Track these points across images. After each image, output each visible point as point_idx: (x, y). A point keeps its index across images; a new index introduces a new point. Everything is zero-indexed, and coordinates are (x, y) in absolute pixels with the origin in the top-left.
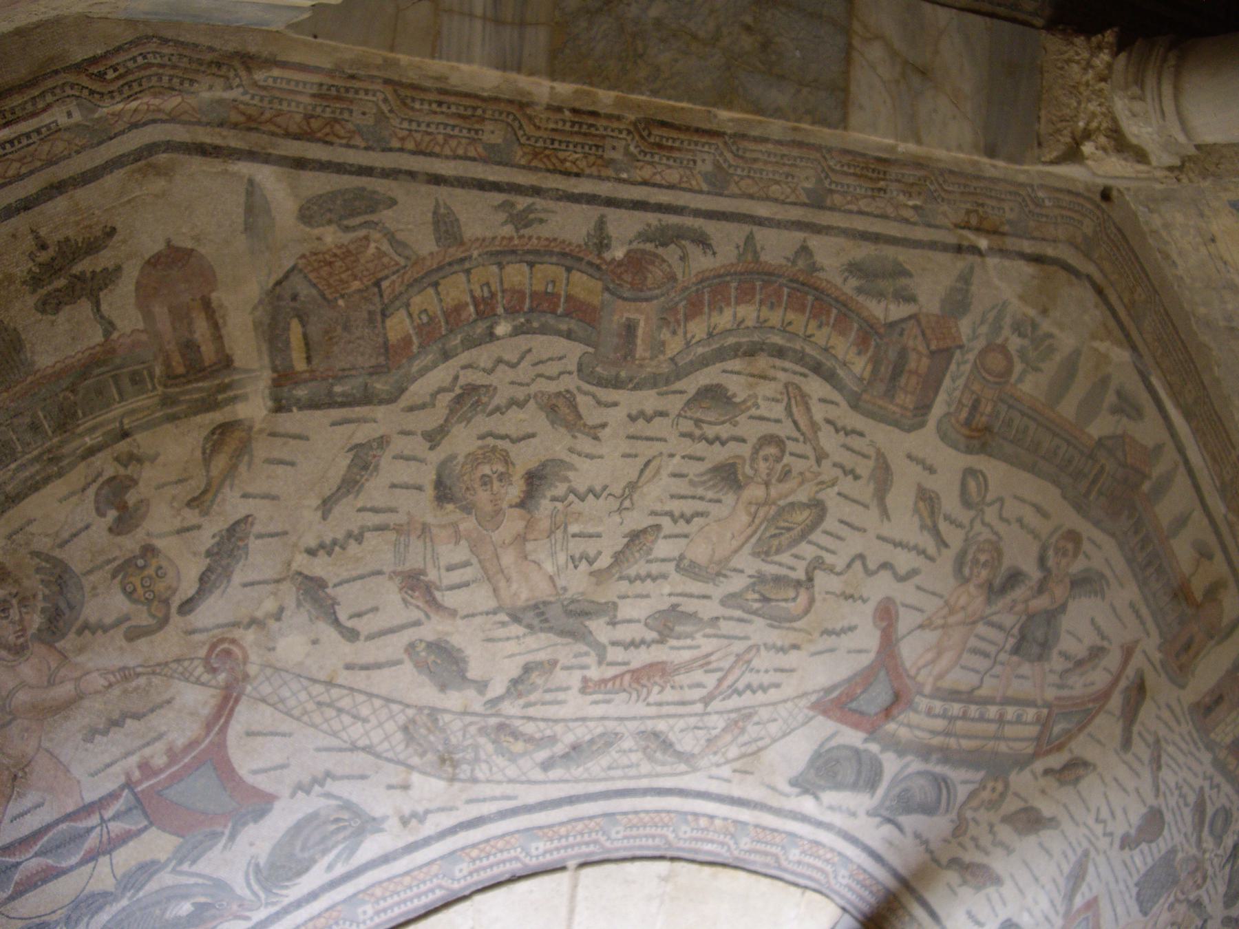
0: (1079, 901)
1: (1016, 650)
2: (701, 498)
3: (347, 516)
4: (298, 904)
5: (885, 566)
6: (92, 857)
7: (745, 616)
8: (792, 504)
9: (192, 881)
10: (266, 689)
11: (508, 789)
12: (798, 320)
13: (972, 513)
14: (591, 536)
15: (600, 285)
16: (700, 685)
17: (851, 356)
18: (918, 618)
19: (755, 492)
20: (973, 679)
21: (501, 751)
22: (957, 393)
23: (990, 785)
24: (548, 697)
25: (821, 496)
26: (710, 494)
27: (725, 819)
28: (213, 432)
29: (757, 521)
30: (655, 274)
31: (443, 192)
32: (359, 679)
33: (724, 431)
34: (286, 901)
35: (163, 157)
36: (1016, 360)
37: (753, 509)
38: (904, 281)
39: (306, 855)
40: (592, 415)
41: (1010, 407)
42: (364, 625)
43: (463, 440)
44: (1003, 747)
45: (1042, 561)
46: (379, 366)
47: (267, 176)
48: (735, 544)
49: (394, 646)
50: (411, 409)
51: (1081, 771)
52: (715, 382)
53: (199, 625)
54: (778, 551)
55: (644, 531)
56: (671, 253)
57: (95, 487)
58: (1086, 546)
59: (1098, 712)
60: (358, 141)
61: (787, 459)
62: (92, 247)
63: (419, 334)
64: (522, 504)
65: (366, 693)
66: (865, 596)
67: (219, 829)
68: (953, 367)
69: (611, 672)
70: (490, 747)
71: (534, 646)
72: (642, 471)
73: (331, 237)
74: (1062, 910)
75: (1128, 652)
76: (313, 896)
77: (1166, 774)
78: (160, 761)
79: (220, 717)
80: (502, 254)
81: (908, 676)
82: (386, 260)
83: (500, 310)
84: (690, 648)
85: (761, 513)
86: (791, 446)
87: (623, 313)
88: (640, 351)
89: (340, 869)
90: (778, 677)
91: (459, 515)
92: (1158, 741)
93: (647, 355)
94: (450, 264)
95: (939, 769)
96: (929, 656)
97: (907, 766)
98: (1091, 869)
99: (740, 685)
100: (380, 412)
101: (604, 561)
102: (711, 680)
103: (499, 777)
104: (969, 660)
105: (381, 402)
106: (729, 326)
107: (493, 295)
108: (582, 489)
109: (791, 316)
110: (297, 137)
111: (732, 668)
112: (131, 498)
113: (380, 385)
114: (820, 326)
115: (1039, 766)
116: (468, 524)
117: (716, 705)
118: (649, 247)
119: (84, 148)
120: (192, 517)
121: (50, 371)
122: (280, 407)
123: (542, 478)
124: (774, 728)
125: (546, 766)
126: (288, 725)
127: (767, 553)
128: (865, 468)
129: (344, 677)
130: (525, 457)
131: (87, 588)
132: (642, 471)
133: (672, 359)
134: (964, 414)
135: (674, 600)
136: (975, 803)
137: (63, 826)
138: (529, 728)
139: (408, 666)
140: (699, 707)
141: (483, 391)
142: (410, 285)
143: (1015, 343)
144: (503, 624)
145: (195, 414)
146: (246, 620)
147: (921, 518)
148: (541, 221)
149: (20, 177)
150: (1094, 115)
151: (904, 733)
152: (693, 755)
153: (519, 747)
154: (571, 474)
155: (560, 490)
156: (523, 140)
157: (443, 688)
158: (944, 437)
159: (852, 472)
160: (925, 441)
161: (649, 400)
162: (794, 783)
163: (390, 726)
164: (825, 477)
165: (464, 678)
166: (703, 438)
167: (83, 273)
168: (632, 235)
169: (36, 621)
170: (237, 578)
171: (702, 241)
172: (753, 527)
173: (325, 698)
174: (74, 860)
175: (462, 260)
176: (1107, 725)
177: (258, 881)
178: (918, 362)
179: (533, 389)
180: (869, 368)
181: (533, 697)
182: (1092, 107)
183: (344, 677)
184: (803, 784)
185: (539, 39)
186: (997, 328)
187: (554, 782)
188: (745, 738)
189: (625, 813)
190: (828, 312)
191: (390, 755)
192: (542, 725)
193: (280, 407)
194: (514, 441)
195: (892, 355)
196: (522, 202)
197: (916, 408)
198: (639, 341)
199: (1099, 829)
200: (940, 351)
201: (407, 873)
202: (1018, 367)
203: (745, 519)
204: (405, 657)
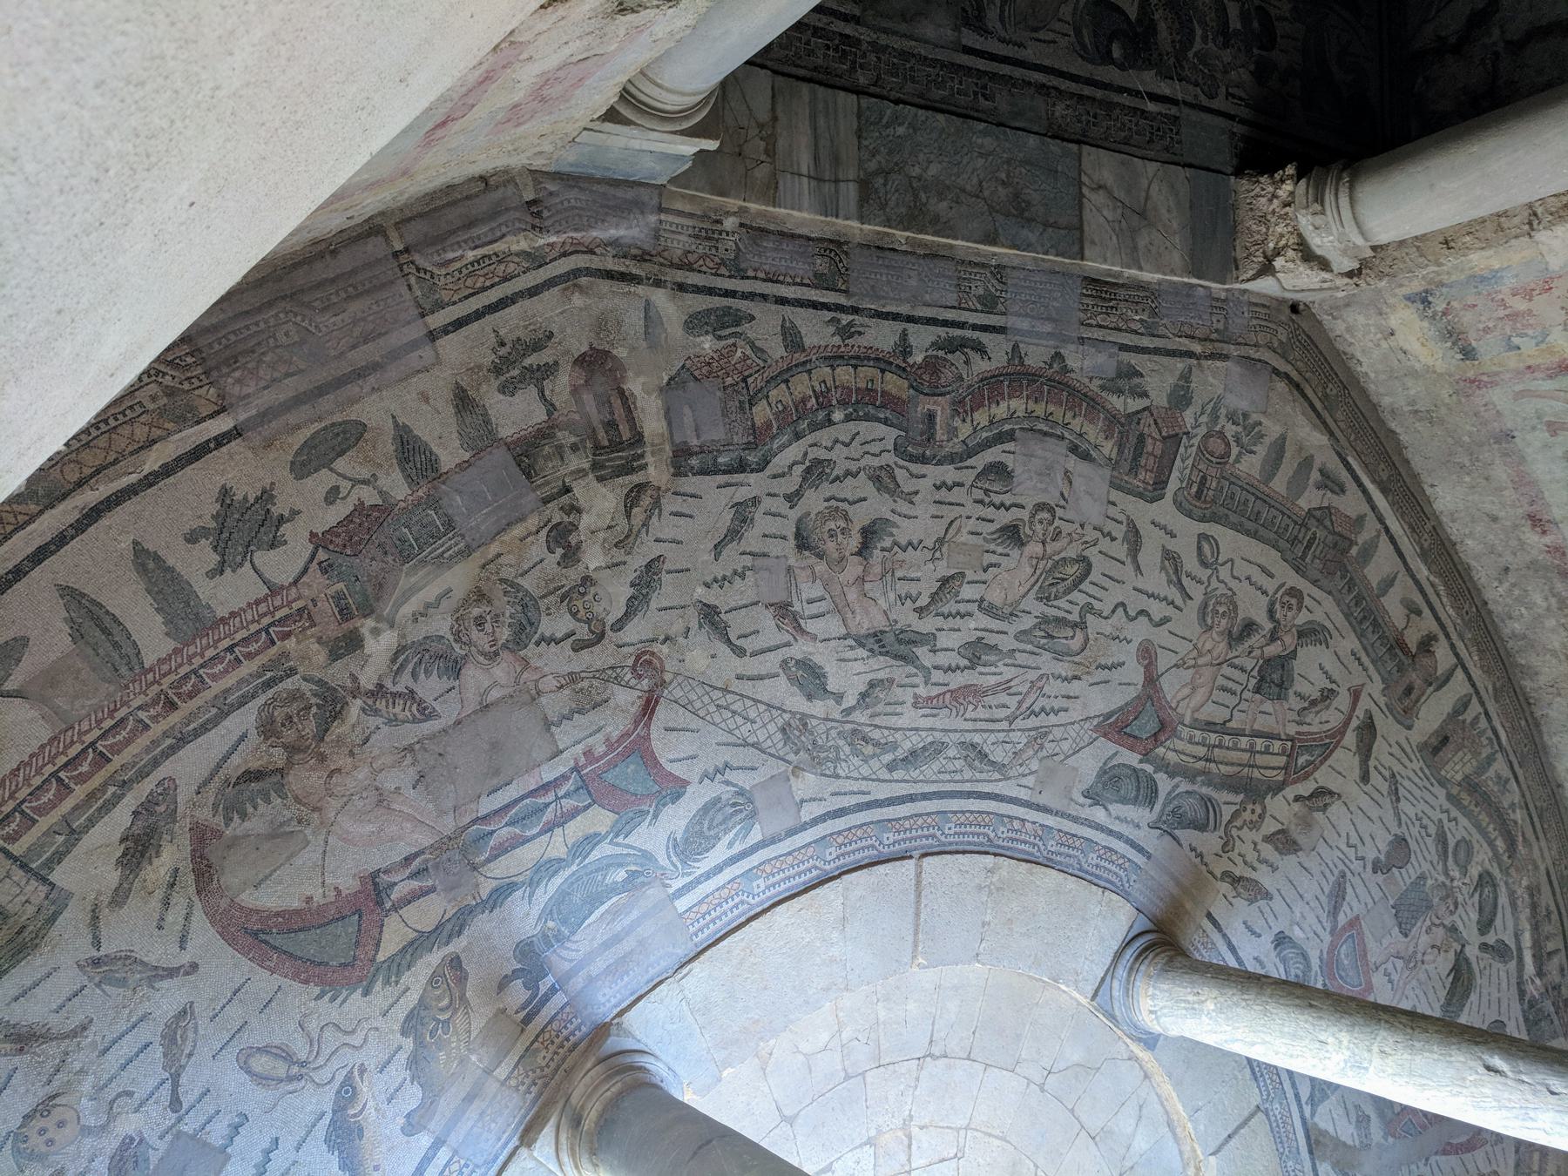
0: (1342, 919)
1: (1257, 690)
2: (994, 552)
3: (732, 558)
4: (708, 876)
5: (1142, 612)
6: (549, 829)
7: (1036, 650)
8: (1064, 559)
9: (625, 851)
10: (678, 693)
11: (864, 785)
12: (1058, 412)
13: (1209, 572)
14: (912, 580)
15: (906, 384)
16: (1004, 706)
17: (1101, 440)
18: (1174, 659)
19: (1034, 548)
20: (1226, 714)
21: (856, 753)
22: (1188, 471)
23: (1250, 807)
24: (889, 709)
25: (1086, 553)
26: (1000, 550)
27: (1034, 823)
28: (631, 491)
29: (1038, 572)
30: (947, 375)
31: (788, 311)
32: (746, 687)
33: (1008, 499)
34: (699, 872)
35: (584, 280)
36: (1233, 444)
37: (1034, 562)
38: (1136, 380)
39: (712, 833)
40: (908, 486)
41: (1232, 483)
42: (749, 644)
43: (814, 501)
45: (1271, 613)
46: (749, 443)
47: (660, 297)
48: (1023, 590)
49: (771, 662)
50: (775, 477)
51: (1327, 799)
52: (997, 460)
53: (628, 640)
54: (1056, 599)
55: (952, 577)
56: (957, 358)
57: (547, 529)
58: (1307, 601)
59: (1335, 748)
60: (723, 271)
61: (1057, 523)
62: (537, 346)
63: (777, 419)
64: (859, 553)
65: (753, 700)
66: (1129, 638)
67: (645, 808)
68: (1182, 450)
69: (935, 691)
70: (847, 749)
71: (876, 667)
72: (947, 530)
73: (707, 344)
74: (1328, 926)
75: (1356, 695)
76: (719, 869)
77: (1403, 805)
78: (600, 749)
79: (644, 715)
80: (834, 359)
81: (1171, 707)
82: (749, 362)
83: (834, 402)
84: (995, 674)
85: (1041, 566)
86: (1059, 512)
87: (926, 405)
88: (940, 434)
89: (738, 848)
90: (1064, 703)
91: (813, 560)
92: (1393, 776)
93: (945, 438)
94: (796, 366)
95: (1205, 790)
96: (1186, 691)
97: (1177, 786)
98: (1349, 890)
99: (1036, 708)
100: (752, 478)
101: (924, 601)
102: (1013, 702)
103: (856, 775)
104: (1219, 696)
105: (752, 471)
106: (1004, 416)
107: (829, 390)
108: (903, 542)
109: (1051, 408)
110: (679, 267)
111: (1028, 693)
112: (573, 539)
113: (752, 458)
114: (1074, 417)
115: (1290, 792)
116: (821, 567)
117: (1019, 723)
118: (941, 353)
119: (528, 269)
120: (619, 555)
121: (509, 440)
122: (679, 472)
123: (875, 532)
124: (1065, 746)
125: (891, 767)
126: (695, 723)
127: (1048, 599)
128: (1119, 531)
129: (736, 686)
130: (861, 516)
131: (543, 608)
132: (947, 530)
133: (963, 442)
134: (1194, 489)
135: (980, 634)
136: (1238, 823)
137: (527, 801)
138: (876, 734)
139: (783, 679)
140: (1005, 725)
141: (826, 464)
142: (768, 382)
143: (1230, 430)
144: (852, 648)
145: (618, 476)
146: (662, 638)
147: (1167, 574)
148: (860, 333)
149: (484, 289)
150: (1282, 236)
151: (1172, 757)
152: (1004, 765)
153: (869, 750)
154: (894, 530)
155: (887, 542)
156: (843, 271)
157: (810, 697)
158: (1179, 505)
159: (1109, 534)
160: (1164, 510)
161: (949, 473)
162: (1086, 794)
163: (772, 728)
164: (1087, 538)
165: (825, 690)
166: (992, 504)
167: (531, 365)
168: (927, 345)
169: (505, 634)
170: (654, 605)
171: (980, 349)
172: (1036, 577)
173: (722, 702)
174: (535, 831)
175: (805, 363)
176: (1345, 758)
177: (677, 855)
178: (1153, 447)
179: (863, 463)
180: (1115, 450)
181: (880, 708)
182: (1279, 229)
183: (736, 686)
184: (1093, 797)
185: (850, 192)
186: (1215, 417)
187: (897, 781)
188: (1044, 753)
189: (955, 813)
190: (1080, 405)
191: (772, 751)
192: (886, 732)
193: (679, 472)
194: (851, 503)
195: (1133, 440)
196: (845, 319)
197: (1155, 483)
198: (938, 427)
199: (1351, 853)
200: (1170, 437)
201: (790, 853)
202: (1235, 450)
203: (1029, 570)
204: (781, 671)
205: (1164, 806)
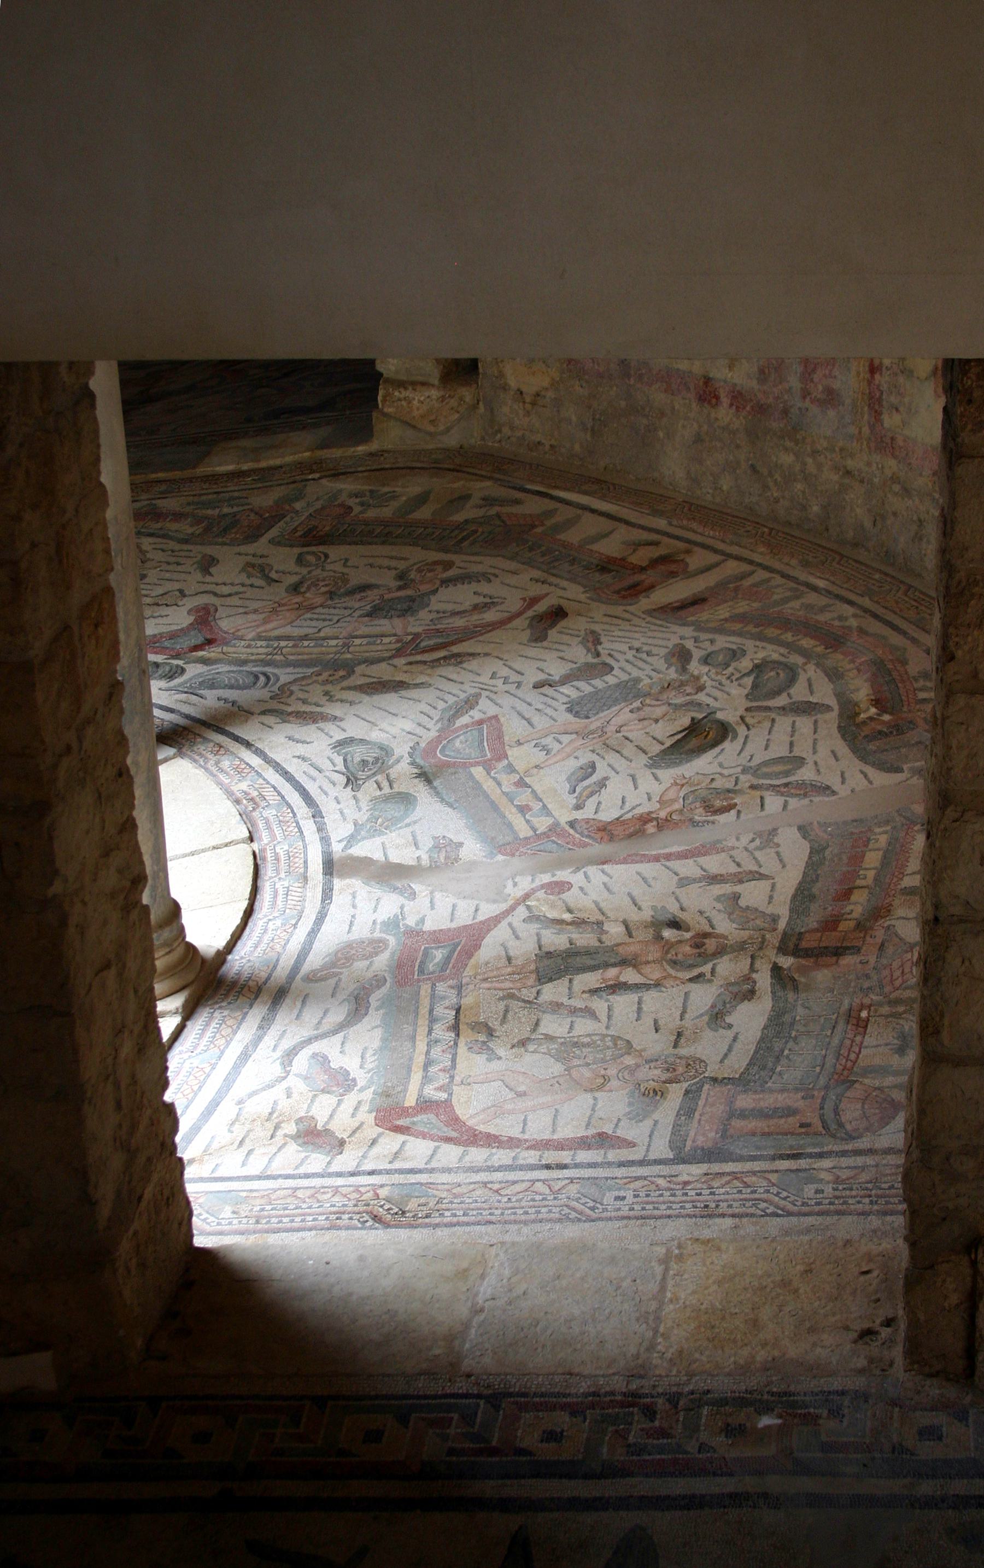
44: (349, 656)
58: (458, 563)
202: (357, 509)
205: (191, 679)
